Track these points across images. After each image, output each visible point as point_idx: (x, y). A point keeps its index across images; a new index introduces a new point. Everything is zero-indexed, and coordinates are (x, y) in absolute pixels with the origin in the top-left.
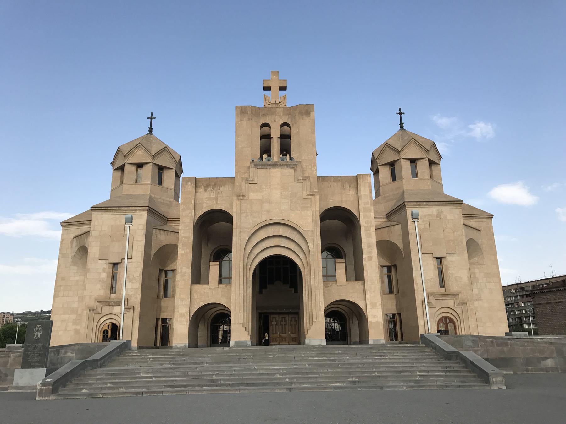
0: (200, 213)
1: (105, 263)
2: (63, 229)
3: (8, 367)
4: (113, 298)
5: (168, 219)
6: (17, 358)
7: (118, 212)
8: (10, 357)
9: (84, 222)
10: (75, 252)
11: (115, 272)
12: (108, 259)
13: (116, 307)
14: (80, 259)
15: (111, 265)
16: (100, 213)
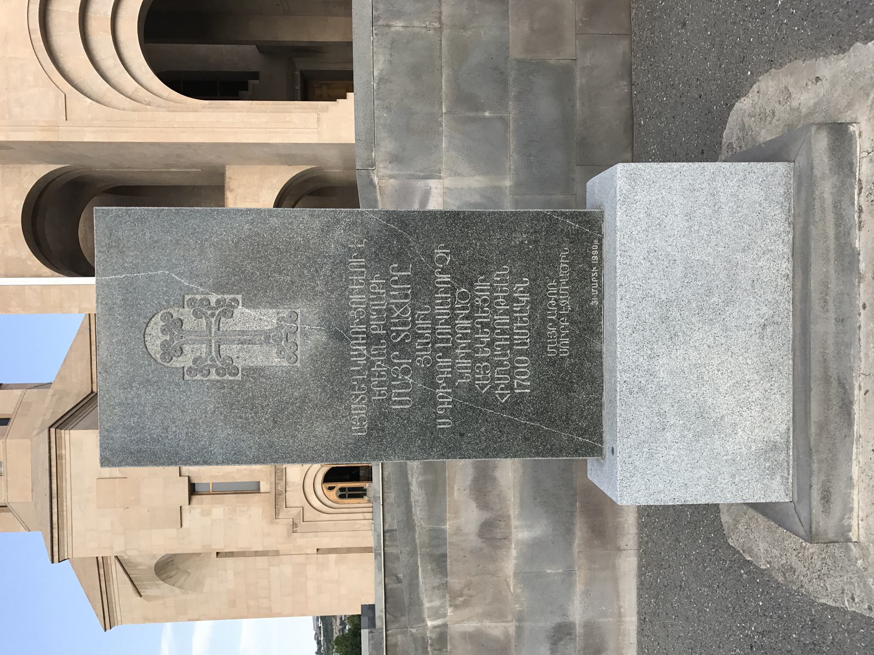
0: (35, 263)
1: (190, 512)
2: (120, 623)
3: (512, 628)
4: (269, 487)
5: (92, 392)
6: (455, 582)
7: (64, 499)
8: (445, 625)
9: (102, 578)
10: (172, 587)
11: (211, 490)
12: (181, 507)
13: (288, 477)
14: (189, 574)
15: (195, 498)
16: (67, 539)
